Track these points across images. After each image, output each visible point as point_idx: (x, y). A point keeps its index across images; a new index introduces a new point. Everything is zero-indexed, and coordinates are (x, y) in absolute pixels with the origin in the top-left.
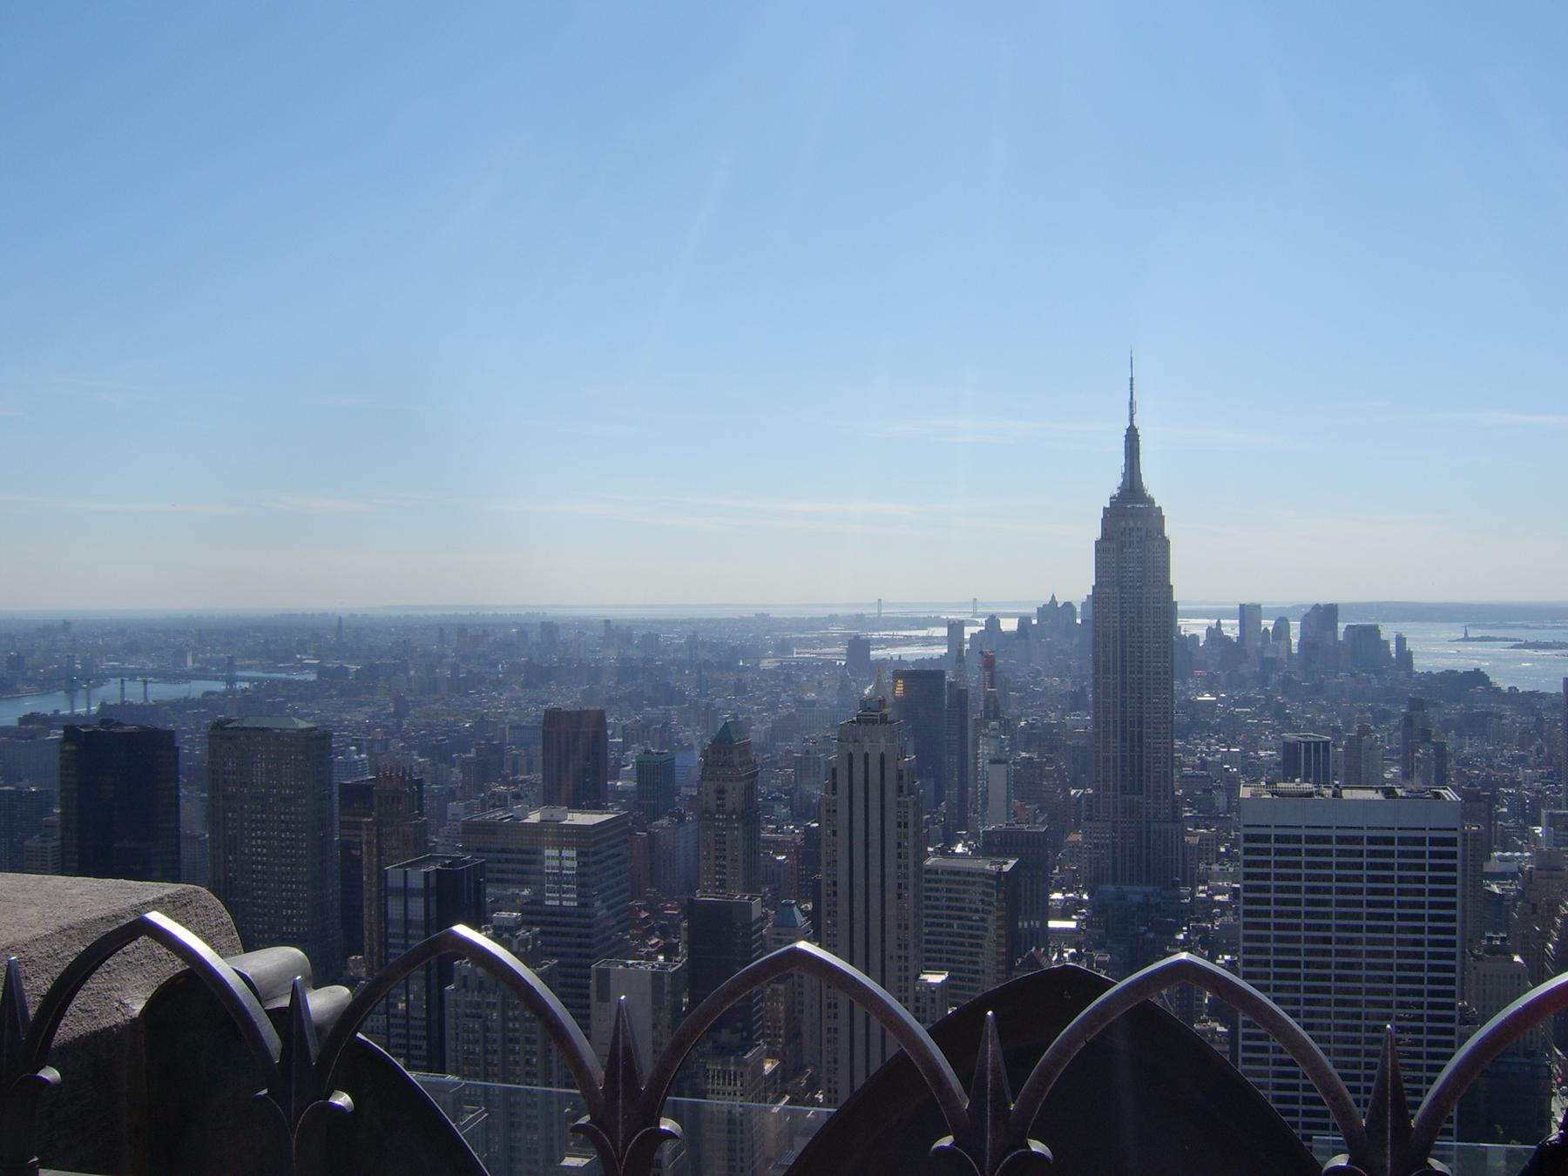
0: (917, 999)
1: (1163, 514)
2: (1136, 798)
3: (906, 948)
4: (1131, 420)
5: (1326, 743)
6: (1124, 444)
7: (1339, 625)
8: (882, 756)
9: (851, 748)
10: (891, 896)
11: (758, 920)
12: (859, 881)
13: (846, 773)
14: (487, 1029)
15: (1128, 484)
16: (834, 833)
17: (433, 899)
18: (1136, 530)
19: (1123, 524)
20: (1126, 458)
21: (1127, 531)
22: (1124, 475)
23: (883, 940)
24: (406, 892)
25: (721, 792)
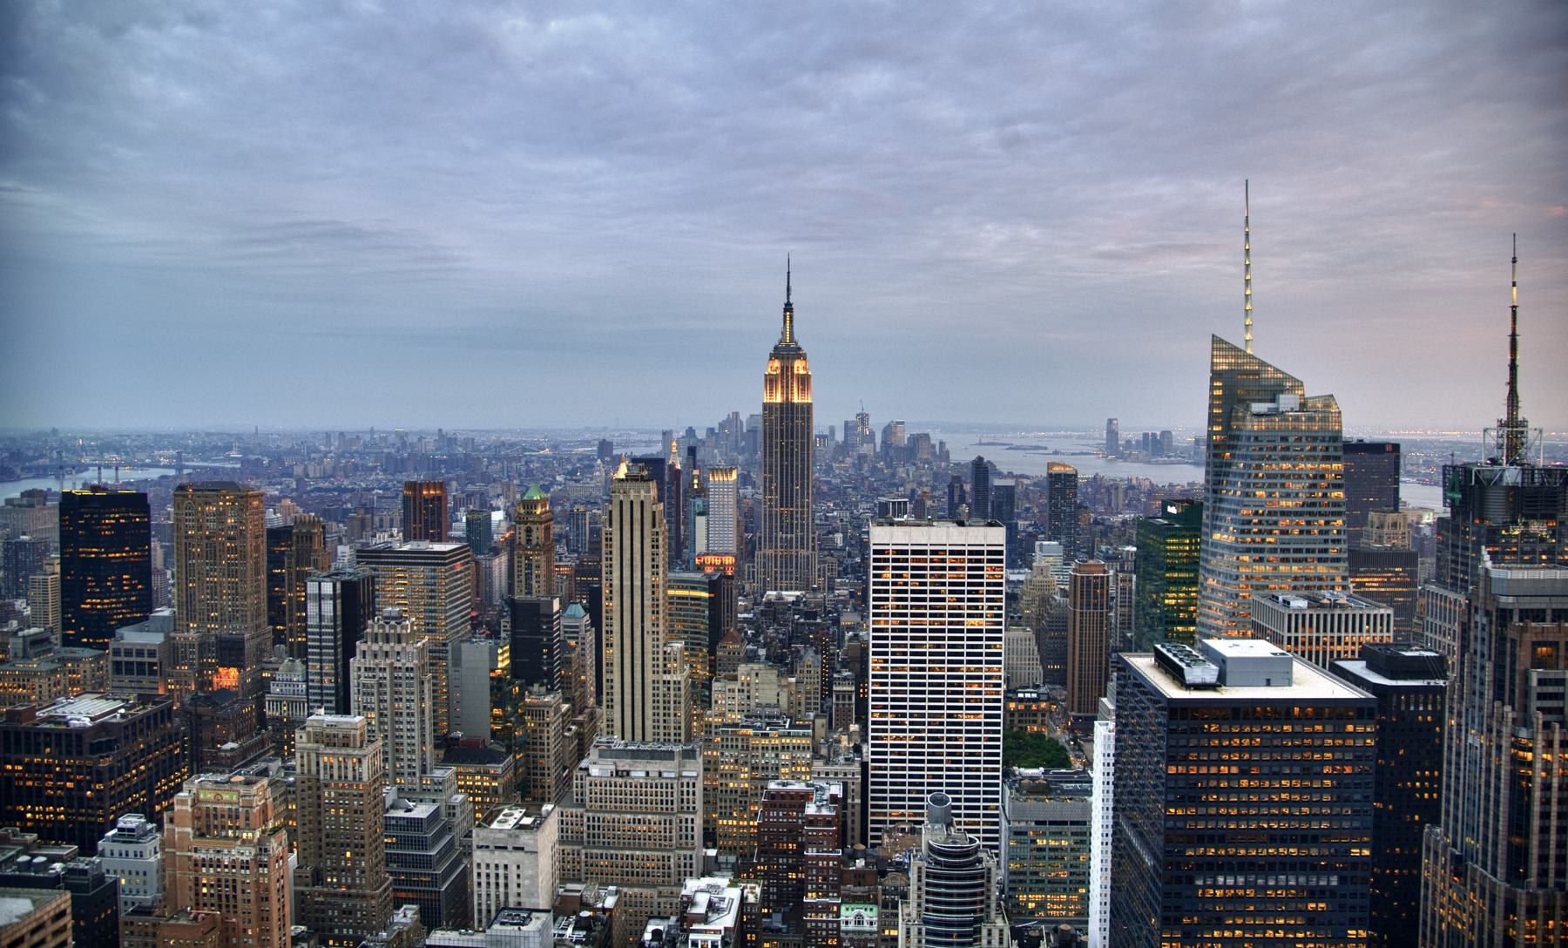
0: (665, 659)
3: (658, 626)
5: (905, 503)
8: (642, 502)
9: (622, 498)
10: (648, 593)
11: (558, 612)
12: (627, 583)
13: (619, 513)
14: (380, 685)
16: (611, 553)
17: (339, 601)
23: (643, 621)
24: (320, 597)
25: (529, 531)
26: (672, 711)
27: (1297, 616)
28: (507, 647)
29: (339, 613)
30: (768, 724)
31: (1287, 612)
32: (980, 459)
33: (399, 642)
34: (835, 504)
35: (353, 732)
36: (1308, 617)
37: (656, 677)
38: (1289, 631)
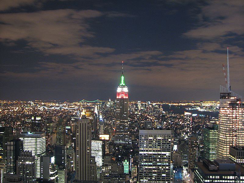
10: (87, 145)
12: (82, 142)
26: (92, 173)
27: (240, 152)
28: (54, 157)
29: (15, 149)
30: (115, 176)
31: (237, 151)
33: (28, 156)
35: (16, 178)
36: (242, 152)
37: (88, 165)
38: (238, 156)
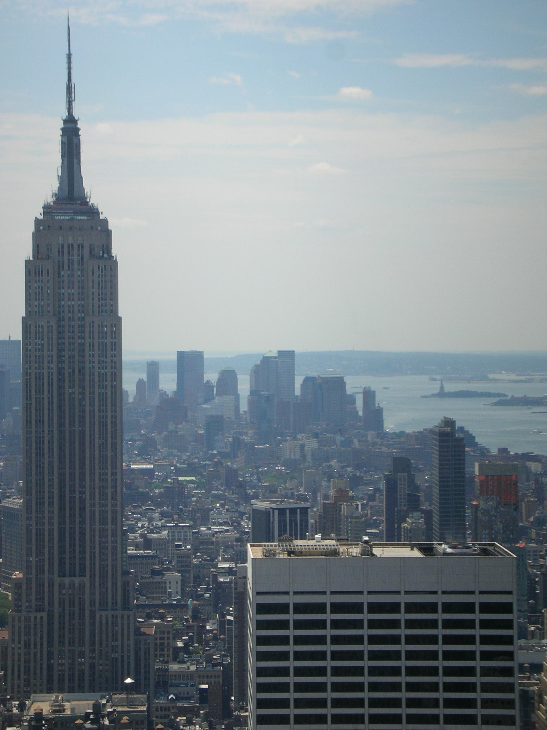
1: (110, 228)
2: (77, 580)
4: (70, 108)
5: (304, 511)
6: (61, 137)
7: (296, 377)
15: (67, 189)
18: (75, 246)
19: (60, 239)
20: (63, 156)
21: (66, 251)
22: (61, 179)
32: (449, 423)
34: (163, 515)
